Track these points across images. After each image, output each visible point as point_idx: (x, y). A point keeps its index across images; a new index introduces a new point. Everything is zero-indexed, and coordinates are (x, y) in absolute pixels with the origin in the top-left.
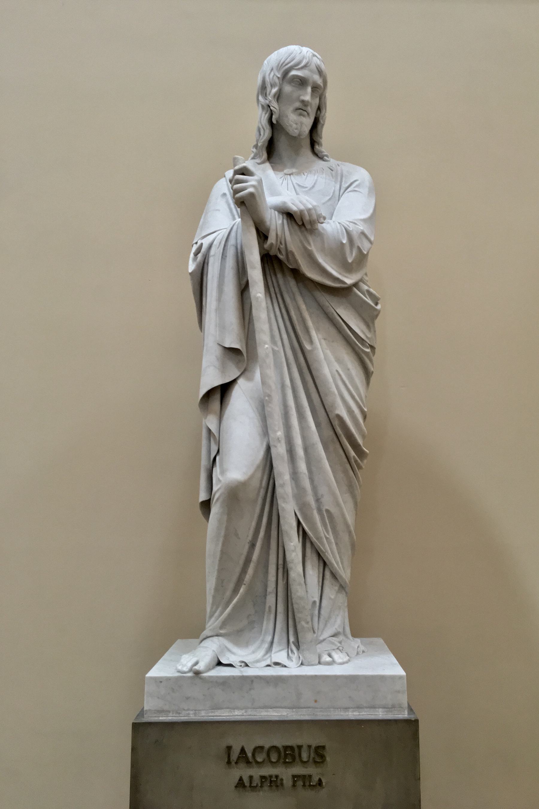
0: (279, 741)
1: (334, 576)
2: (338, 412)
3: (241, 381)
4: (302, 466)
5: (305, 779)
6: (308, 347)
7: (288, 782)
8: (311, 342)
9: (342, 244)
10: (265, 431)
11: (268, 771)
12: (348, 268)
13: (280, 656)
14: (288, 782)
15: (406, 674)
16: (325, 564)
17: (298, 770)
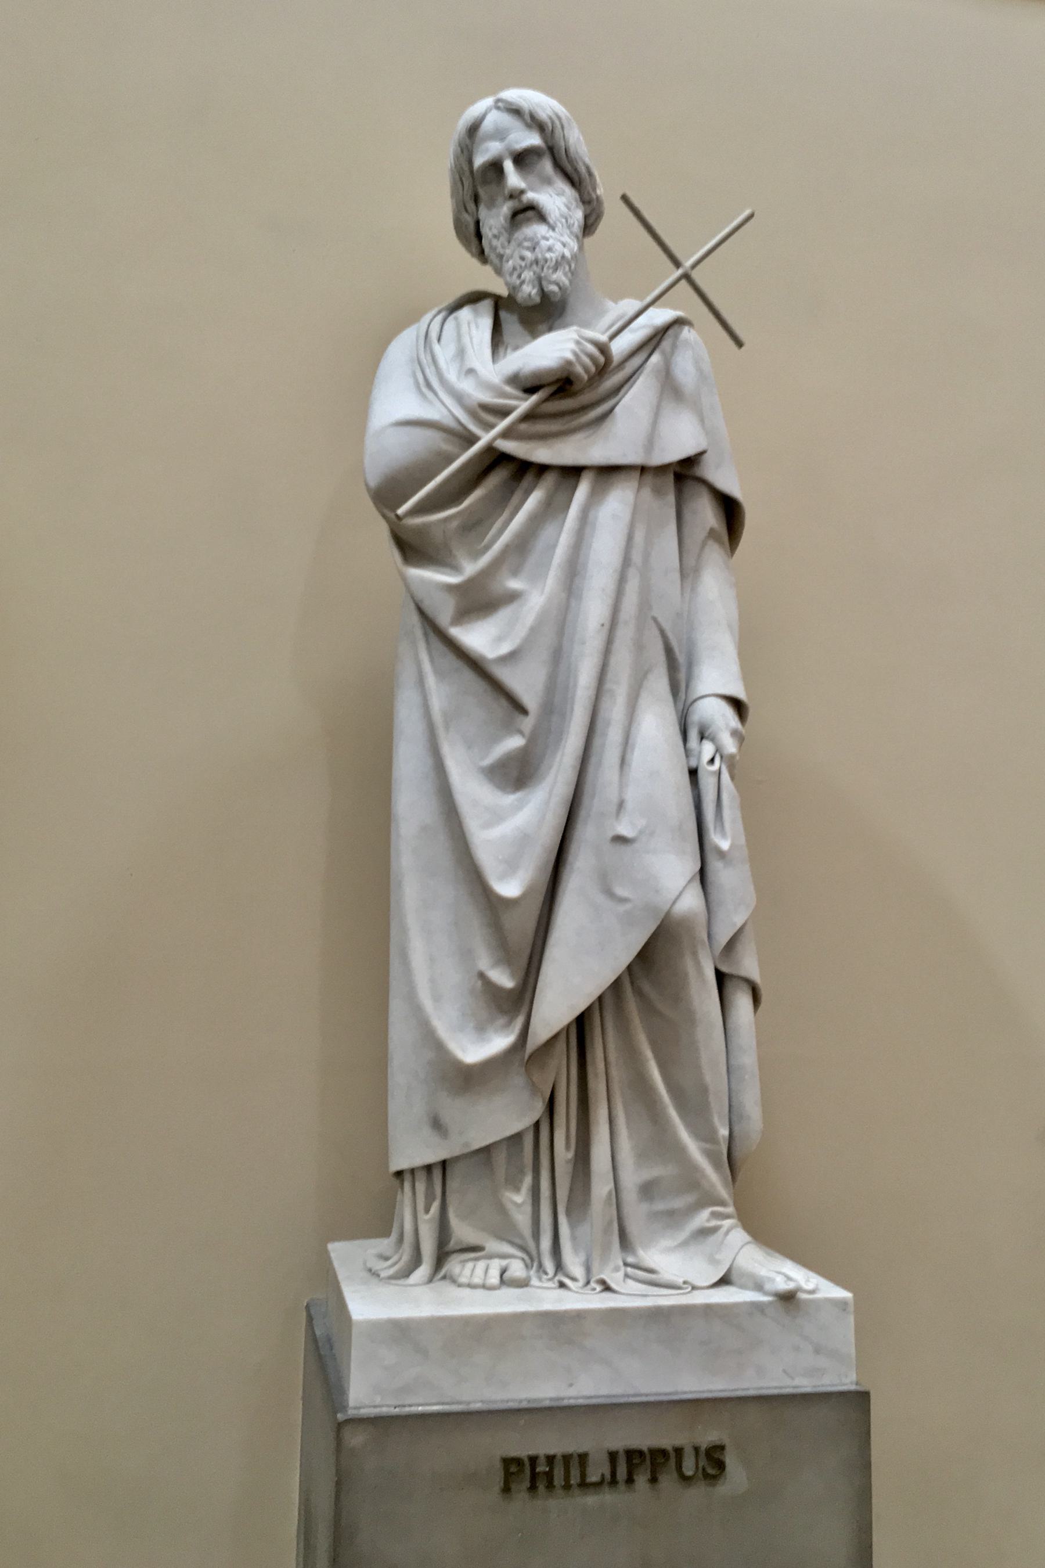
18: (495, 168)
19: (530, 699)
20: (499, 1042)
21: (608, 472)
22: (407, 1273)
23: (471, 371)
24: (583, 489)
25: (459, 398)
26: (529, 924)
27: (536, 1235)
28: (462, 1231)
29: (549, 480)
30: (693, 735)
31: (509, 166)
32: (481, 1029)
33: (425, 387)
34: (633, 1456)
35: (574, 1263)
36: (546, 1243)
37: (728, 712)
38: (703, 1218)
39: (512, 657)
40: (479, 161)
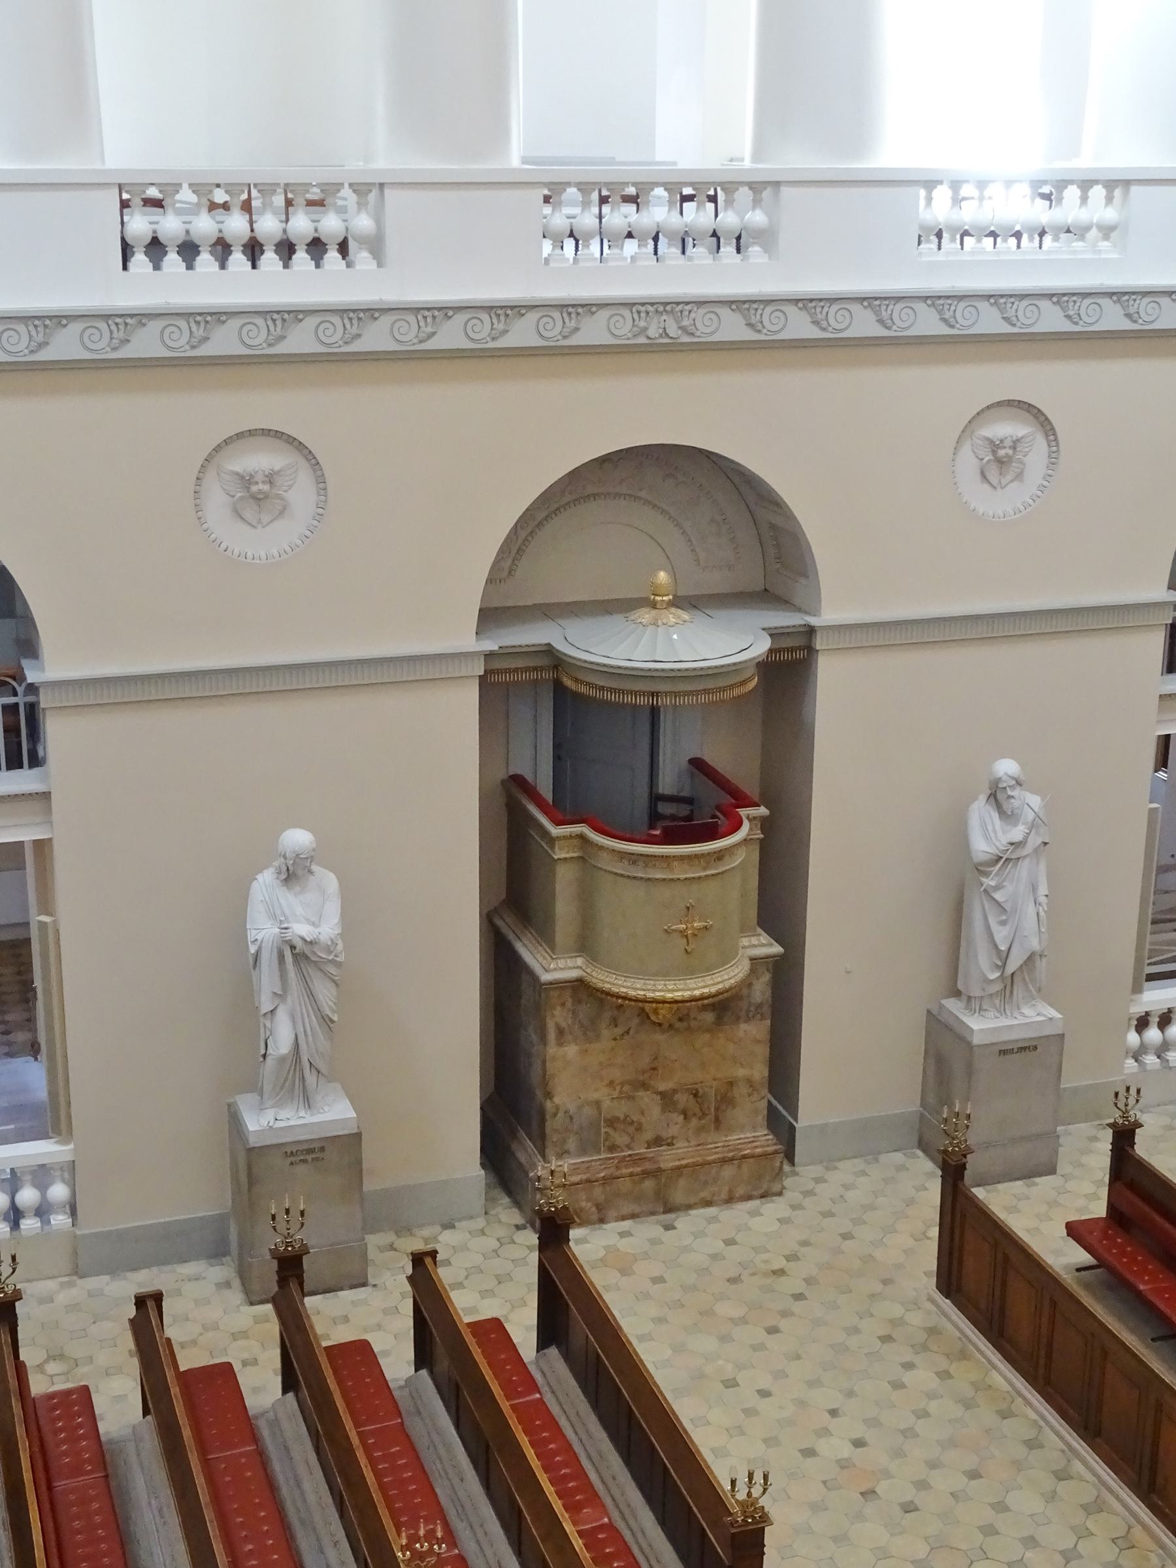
0: (305, 1147)
1: (323, 1075)
2: (326, 1013)
3: (281, 1005)
4: (310, 1038)
5: (317, 1159)
6: (311, 986)
7: (310, 1160)
8: (314, 985)
9: (328, 945)
10: (295, 1028)
11: (302, 1158)
12: (330, 952)
13: (302, 1113)
14: (310, 1160)
15: (315, 836)
16: (319, 1072)
17: (314, 1156)
18: (1005, 788)
19: (1008, 909)
20: (997, 974)
21: (1025, 857)
22: (973, 1015)
23: (999, 840)
24: (1020, 860)
25: (998, 848)
26: (1005, 954)
27: (1000, 1006)
28: (985, 1007)
29: (1013, 860)
30: (1037, 904)
31: (1008, 788)
32: (993, 971)
33: (987, 838)
34: (1022, 1048)
35: (1009, 1014)
36: (1002, 1010)
37: (1045, 898)
38: (1033, 1002)
39: (1005, 901)
40: (1000, 786)
